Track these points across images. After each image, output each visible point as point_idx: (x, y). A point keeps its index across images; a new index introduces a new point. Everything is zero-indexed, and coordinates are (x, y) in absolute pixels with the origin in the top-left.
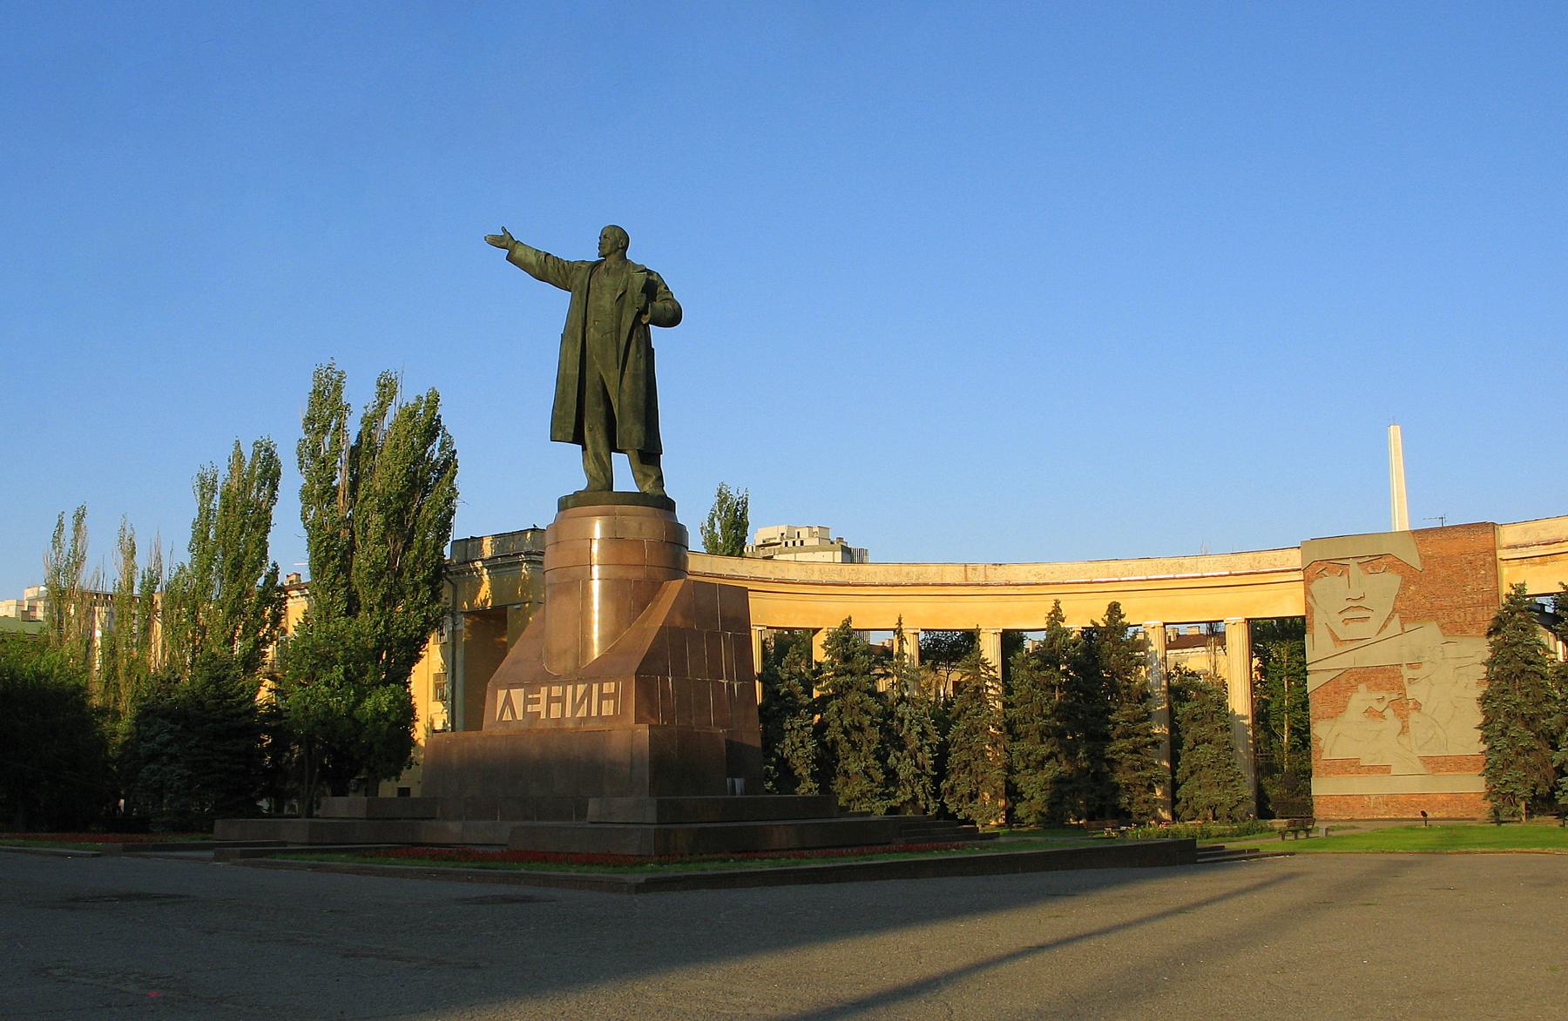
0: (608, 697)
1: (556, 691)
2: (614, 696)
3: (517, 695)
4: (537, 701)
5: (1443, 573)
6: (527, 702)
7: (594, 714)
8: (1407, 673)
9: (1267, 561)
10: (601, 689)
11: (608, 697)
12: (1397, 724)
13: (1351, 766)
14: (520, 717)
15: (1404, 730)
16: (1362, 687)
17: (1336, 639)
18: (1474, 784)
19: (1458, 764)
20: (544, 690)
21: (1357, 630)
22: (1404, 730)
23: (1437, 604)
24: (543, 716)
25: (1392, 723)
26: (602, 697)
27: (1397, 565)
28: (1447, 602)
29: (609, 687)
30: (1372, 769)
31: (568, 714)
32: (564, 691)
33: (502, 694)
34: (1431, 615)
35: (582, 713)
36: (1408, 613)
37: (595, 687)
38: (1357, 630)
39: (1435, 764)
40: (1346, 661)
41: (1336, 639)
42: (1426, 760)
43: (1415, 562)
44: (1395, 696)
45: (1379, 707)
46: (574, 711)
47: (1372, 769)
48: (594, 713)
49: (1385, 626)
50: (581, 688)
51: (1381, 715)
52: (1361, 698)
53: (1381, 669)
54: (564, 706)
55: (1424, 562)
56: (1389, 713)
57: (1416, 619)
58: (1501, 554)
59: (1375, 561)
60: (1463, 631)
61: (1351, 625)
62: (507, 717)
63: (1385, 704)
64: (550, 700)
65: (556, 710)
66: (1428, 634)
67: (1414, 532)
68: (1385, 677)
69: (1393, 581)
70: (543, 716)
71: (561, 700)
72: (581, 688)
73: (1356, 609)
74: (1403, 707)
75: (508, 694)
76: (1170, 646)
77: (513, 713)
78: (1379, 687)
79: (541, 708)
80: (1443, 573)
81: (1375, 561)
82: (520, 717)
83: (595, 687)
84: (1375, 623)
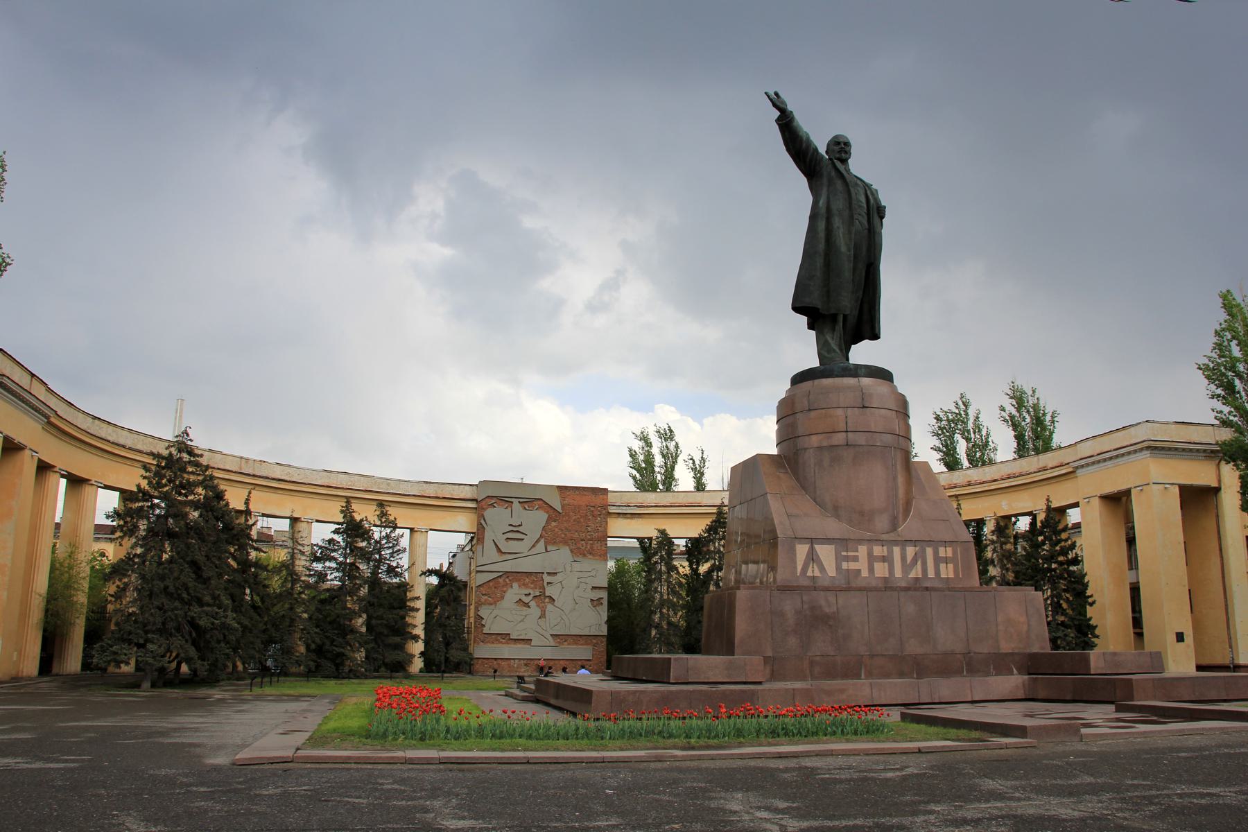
0: (946, 560)
1: (878, 550)
2: (952, 560)
4: (856, 559)
6: (839, 559)
7: (931, 574)
8: (547, 579)
10: (936, 553)
11: (946, 560)
12: (537, 612)
13: (505, 637)
14: (832, 572)
15: (543, 616)
16: (515, 585)
17: (499, 550)
20: (862, 550)
22: (543, 616)
23: (569, 535)
24: (865, 574)
25: (535, 610)
26: (938, 560)
28: (576, 535)
32: (891, 552)
34: (565, 543)
35: (916, 572)
36: (550, 538)
37: (929, 551)
40: (507, 567)
41: (499, 550)
45: (526, 600)
48: (931, 574)
50: (910, 551)
51: (527, 605)
52: (515, 592)
55: (563, 507)
56: (533, 604)
57: (554, 543)
62: (814, 571)
64: (871, 558)
65: (881, 570)
66: (562, 555)
67: (558, 487)
69: (542, 517)
70: (865, 574)
72: (910, 551)
73: (515, 532)
74: (543, 599)
75: (812, 549)
77: (822, 569)
78: (526, 585)
79: (862, 565)
83: (929, 551)
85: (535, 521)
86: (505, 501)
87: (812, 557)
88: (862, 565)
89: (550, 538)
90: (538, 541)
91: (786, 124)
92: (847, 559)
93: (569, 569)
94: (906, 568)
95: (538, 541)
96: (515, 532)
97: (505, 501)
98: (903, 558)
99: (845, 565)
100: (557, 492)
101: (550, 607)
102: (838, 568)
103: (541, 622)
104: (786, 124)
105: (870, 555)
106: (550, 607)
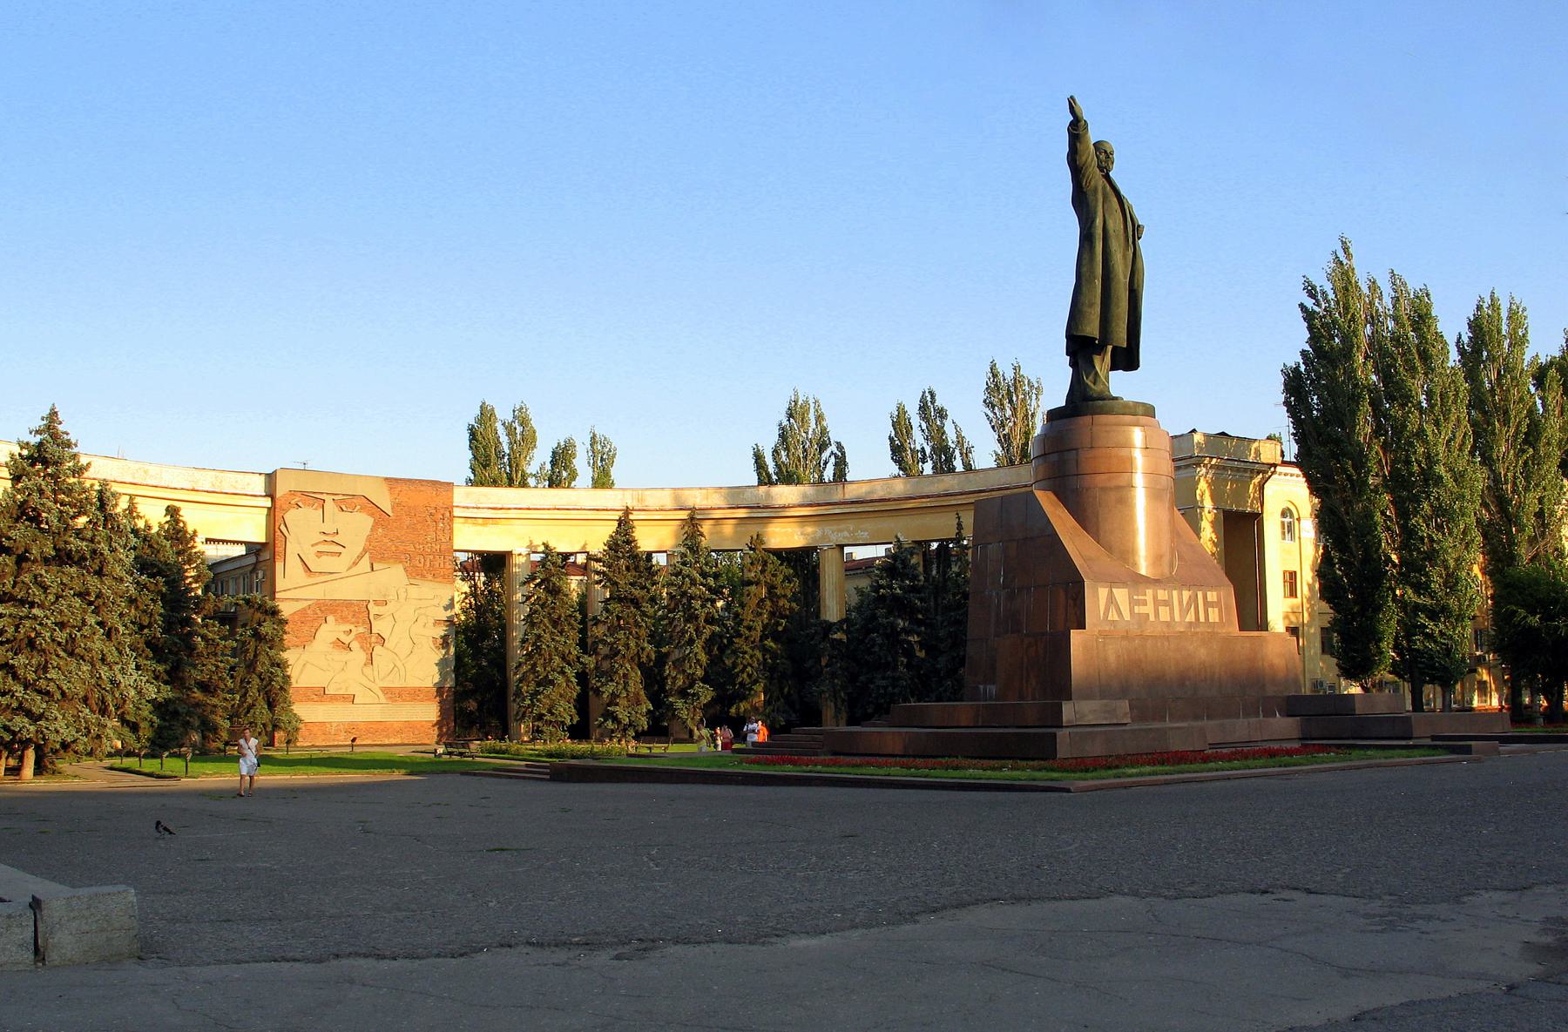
0: (1212, 604)
1: (1162, 594)
3: (1121, 594)
4: (1145, 603)
5: (407, 521)
6: (1133, 603)
7: (1202, 619)
8: (374, 610)
9: (229, 482)
10: (1205, 597)
11: (1212, 604)
13: (321, 695)
14: (1127, 617)
16: (330, 618)
18: (429, 712)
19: (414, 694)
21: (327, 564)
24: (1152, 618)
25: (358, 655)
26: (1207, 604)
27: (370, 506)
29: (1212, 596)
30: (334, 698)
31: (1177, 618)
32: (1171, 596)
33: (1103, 593)
34: (396, 558)
35: (1190, 617)
36: (377, 553)
38: (327, 564)
39: (395, 695)
40: (317, 592)
42: (385, 690)
43: (387, 507)
44: (361, 630)
45: (346, 639)
46: (1183, 616)
47: (334, 698)
48: (1202, 619)
49: (355, 564)
50: (1186, 594)
52: (330, 630)
53: (348, 604)
54: (1172, 610)
57: (382, 559)
58: (456, 512)
59: (348, 502)
60: (423, 576)
61: (324, 558)
62: (1113, 616)
63: (352, 635)
64: (1157, 603)
65: (1164, 614)
66: (392, 576)
68: (358, 612)
70: (1152, 618)
71: (1168, 603)
73: (331, 543)
74: (372, 641)
75: (1111, 595)
76: (1293, 594)
77: (1120, 613)
78: (344, 620)
79: (1148, 609)
80: (407, 521)
81: (348, 502)
82: (1127, 617)
83: (1200, 595)
84: (348, 556)
85: (356, 528)
86: (314, 499)
87: (1111, 599)
88: (1148, 609)
89: (377, 553)
90: (360, 557)
91: (1077, 129)
92: (1139, 603)
93: (402, 596)
94: (1184, 612)
95: (360, 557)
96: (331, 543)
97: (314, 499)
98: (1181, 602)
99: (1137, 609)
100: (385, 488)
101: (378, 649)
102: (1132, 610)
103: (368, 670)
104: (1077, 129)
105: (1155, 598)
106: (378, 649)
